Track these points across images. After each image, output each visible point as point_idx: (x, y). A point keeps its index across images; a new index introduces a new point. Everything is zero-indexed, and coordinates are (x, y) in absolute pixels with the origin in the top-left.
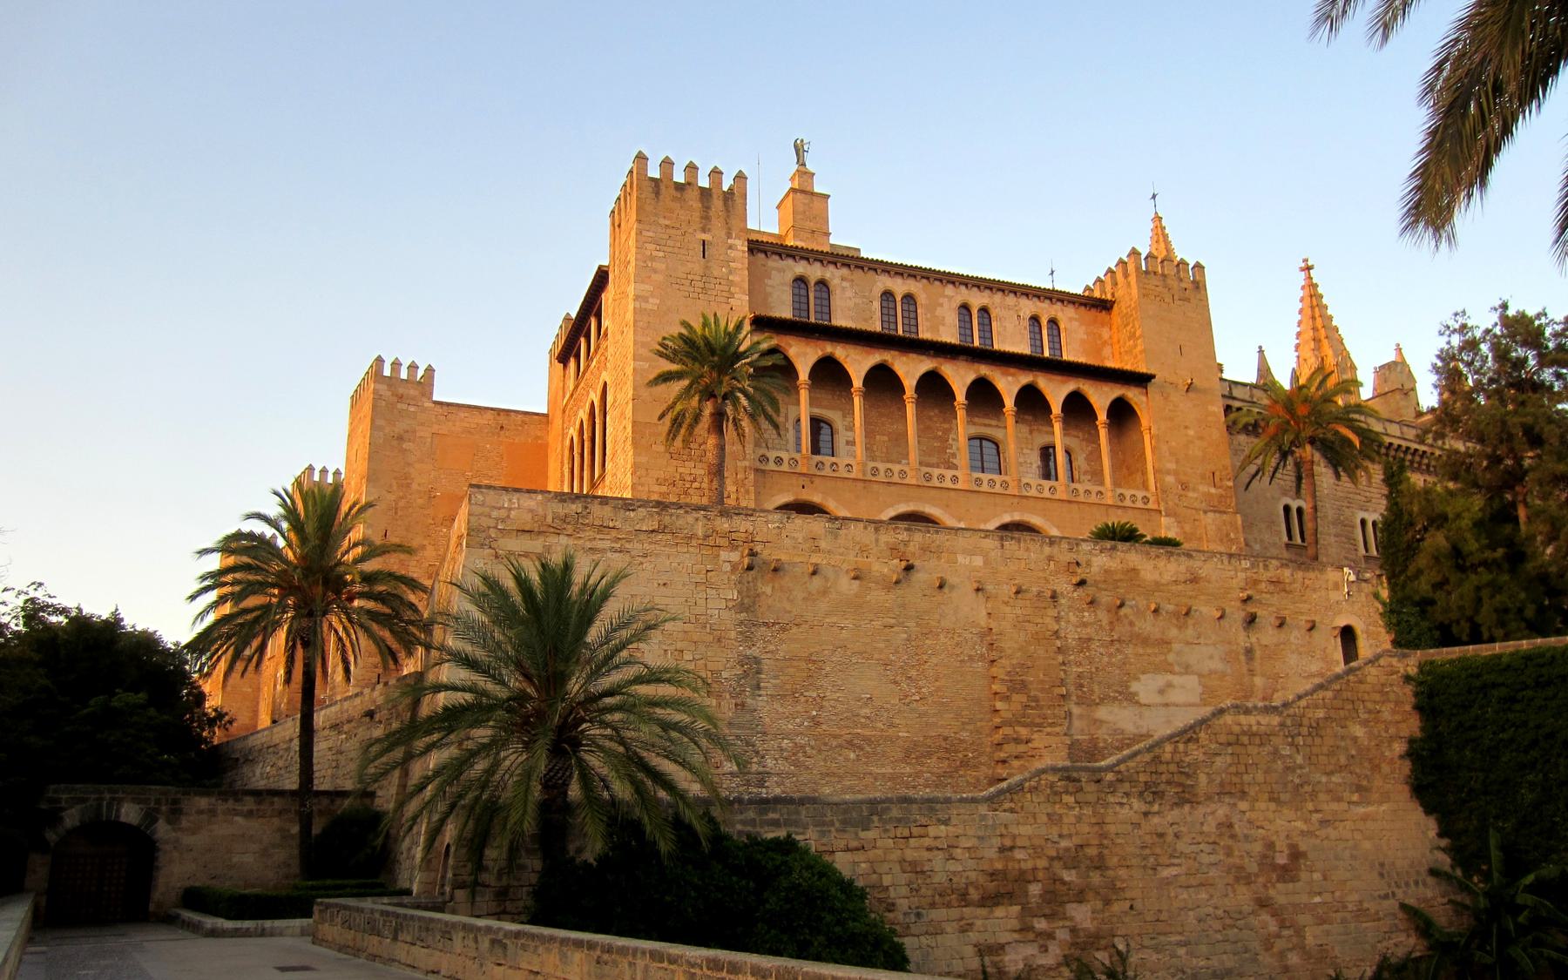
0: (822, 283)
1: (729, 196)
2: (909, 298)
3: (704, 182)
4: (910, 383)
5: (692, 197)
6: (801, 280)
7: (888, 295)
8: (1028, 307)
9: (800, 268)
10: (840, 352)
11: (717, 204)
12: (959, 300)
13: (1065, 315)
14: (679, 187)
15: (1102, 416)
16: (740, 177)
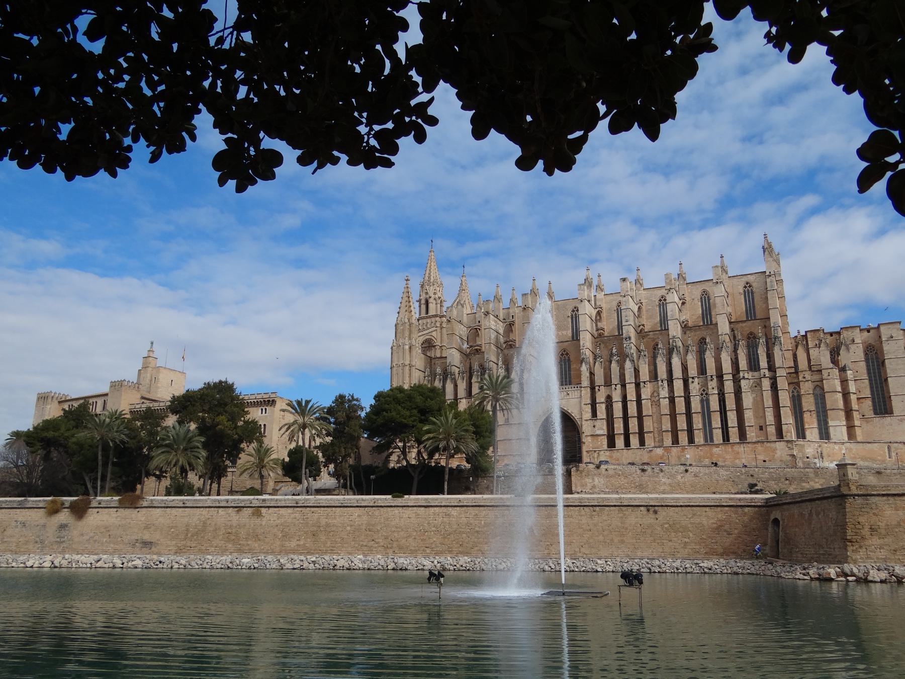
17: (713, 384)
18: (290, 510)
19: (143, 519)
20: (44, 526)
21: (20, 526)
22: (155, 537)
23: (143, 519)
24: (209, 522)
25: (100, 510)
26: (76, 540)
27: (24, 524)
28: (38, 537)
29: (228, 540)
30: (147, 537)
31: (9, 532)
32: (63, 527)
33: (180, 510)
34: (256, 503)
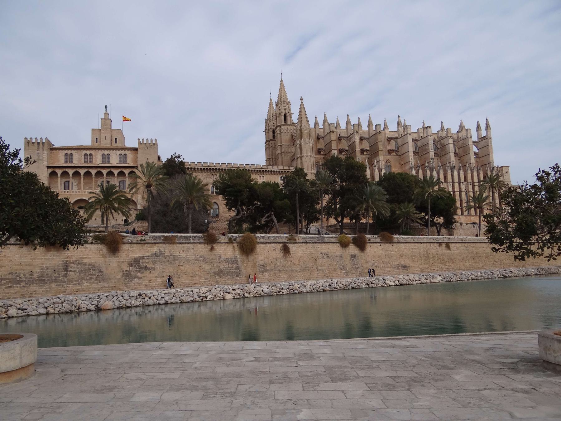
0: (71, 154)
1: (43, 143)
2: (91, 154)
3: (39, 141)
4: (82, 174)
5: (36, 145)
6: (66, 154)
7: (86, 154)
8: (119, 152)
9: (66, 152)
10: (67, 170)
11: (41, 145)
12: (102, 153)
13: (128, 153)
14: (33, 143)
15: (127, 175)
16: (46, 139)
17: (470, 187)
18: (460, 245)
19: (396, 250)
20: (341, 256)
21: (325, 257)
22: (407, 262)
23: (396, 250)
24: (429, 252)
25: (371, 244)
26: (365, 266)
27: (327, 255)
28: (340, 265)
29: (441, 263)
30: (402, 263)
31: (319, 262)
32: (353, 257)
33: (413, 244)
34: (446, 241)
